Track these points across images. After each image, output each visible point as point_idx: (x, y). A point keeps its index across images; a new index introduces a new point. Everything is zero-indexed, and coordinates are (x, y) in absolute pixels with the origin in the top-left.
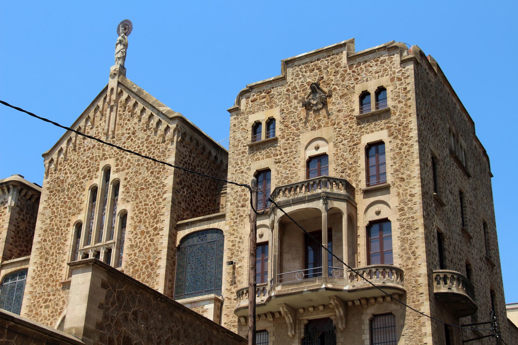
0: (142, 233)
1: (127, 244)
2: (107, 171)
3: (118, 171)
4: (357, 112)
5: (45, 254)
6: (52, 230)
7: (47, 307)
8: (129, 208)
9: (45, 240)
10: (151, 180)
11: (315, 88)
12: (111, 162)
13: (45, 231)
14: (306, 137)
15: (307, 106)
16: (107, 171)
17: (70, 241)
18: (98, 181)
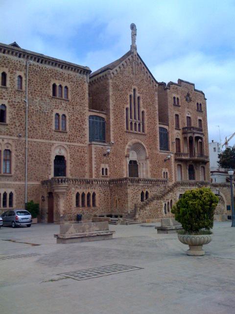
0: (151, 123)
1: (146, 125)
2: (134, 90)
3: (139, 93)
4: (196, 108)
5: (116, 116)
6: (117, 106)
7: (121, 139)
8: (145, 110)
9: (115, 110)
10: (151, 103)
11: (188, 95)
12: (136, 88)
13: (114, 105)
14: (186, 110)
15: (187, 100)
16: (134, 90)
17: (125, 115)
18: (132, 93)
